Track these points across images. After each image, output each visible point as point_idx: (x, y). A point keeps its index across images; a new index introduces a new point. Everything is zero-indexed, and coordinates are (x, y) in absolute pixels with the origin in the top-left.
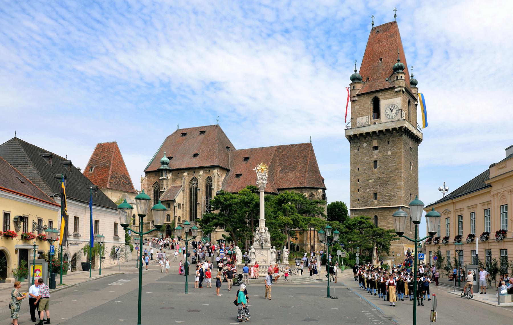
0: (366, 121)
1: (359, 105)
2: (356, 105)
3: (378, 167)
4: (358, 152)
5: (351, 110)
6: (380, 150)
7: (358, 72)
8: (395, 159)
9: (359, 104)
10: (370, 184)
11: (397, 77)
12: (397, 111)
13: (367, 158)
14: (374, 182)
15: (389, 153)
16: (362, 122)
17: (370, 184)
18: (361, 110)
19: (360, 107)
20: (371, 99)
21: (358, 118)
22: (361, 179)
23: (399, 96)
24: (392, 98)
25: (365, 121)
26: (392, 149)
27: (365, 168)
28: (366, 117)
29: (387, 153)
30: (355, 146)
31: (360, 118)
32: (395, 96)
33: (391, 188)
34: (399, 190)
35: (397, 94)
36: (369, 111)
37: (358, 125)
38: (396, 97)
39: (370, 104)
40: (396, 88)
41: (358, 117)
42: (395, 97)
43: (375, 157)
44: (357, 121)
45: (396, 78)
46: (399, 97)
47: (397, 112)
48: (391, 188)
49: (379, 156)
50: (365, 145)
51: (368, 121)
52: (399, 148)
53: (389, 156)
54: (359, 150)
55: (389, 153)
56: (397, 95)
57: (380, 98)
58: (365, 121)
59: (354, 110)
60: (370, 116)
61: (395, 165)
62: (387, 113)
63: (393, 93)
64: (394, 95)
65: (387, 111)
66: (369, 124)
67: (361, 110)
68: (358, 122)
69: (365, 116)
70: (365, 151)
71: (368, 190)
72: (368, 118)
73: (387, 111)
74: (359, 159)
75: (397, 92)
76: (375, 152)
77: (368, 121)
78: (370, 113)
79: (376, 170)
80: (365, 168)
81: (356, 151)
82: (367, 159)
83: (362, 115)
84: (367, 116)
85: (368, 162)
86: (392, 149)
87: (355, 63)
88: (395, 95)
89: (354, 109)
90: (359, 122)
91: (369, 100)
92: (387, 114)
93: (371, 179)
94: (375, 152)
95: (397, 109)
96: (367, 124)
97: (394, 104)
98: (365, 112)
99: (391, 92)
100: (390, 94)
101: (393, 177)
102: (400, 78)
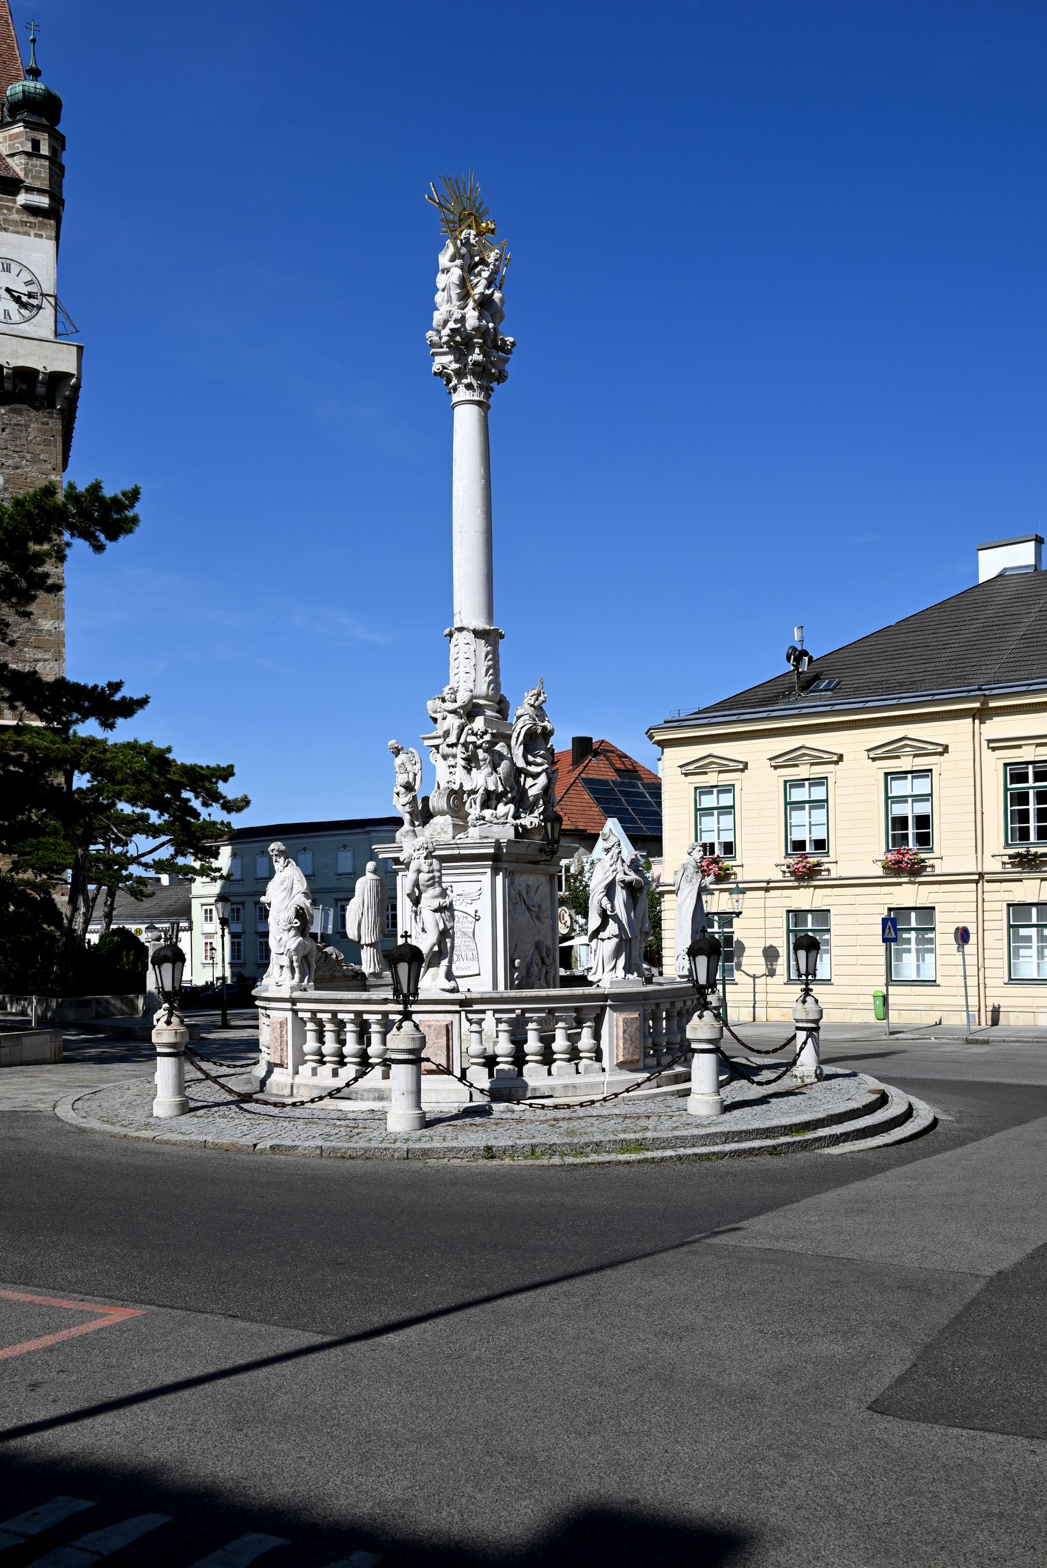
11: (36, 144)
23: (43, 233)
26: (10, 462)
32: (22, 228)
34: (47, 657)
35: (31, 219)
40: (29, 190)
42: (20, 229)
45: (28, 147)
46: (41, 236)
52: (49, 466)
56: (32, 226)
64: (15, 216)
75: (31, 210)
86: (10, 462)
88: (24, 223)
102: (45, 150)
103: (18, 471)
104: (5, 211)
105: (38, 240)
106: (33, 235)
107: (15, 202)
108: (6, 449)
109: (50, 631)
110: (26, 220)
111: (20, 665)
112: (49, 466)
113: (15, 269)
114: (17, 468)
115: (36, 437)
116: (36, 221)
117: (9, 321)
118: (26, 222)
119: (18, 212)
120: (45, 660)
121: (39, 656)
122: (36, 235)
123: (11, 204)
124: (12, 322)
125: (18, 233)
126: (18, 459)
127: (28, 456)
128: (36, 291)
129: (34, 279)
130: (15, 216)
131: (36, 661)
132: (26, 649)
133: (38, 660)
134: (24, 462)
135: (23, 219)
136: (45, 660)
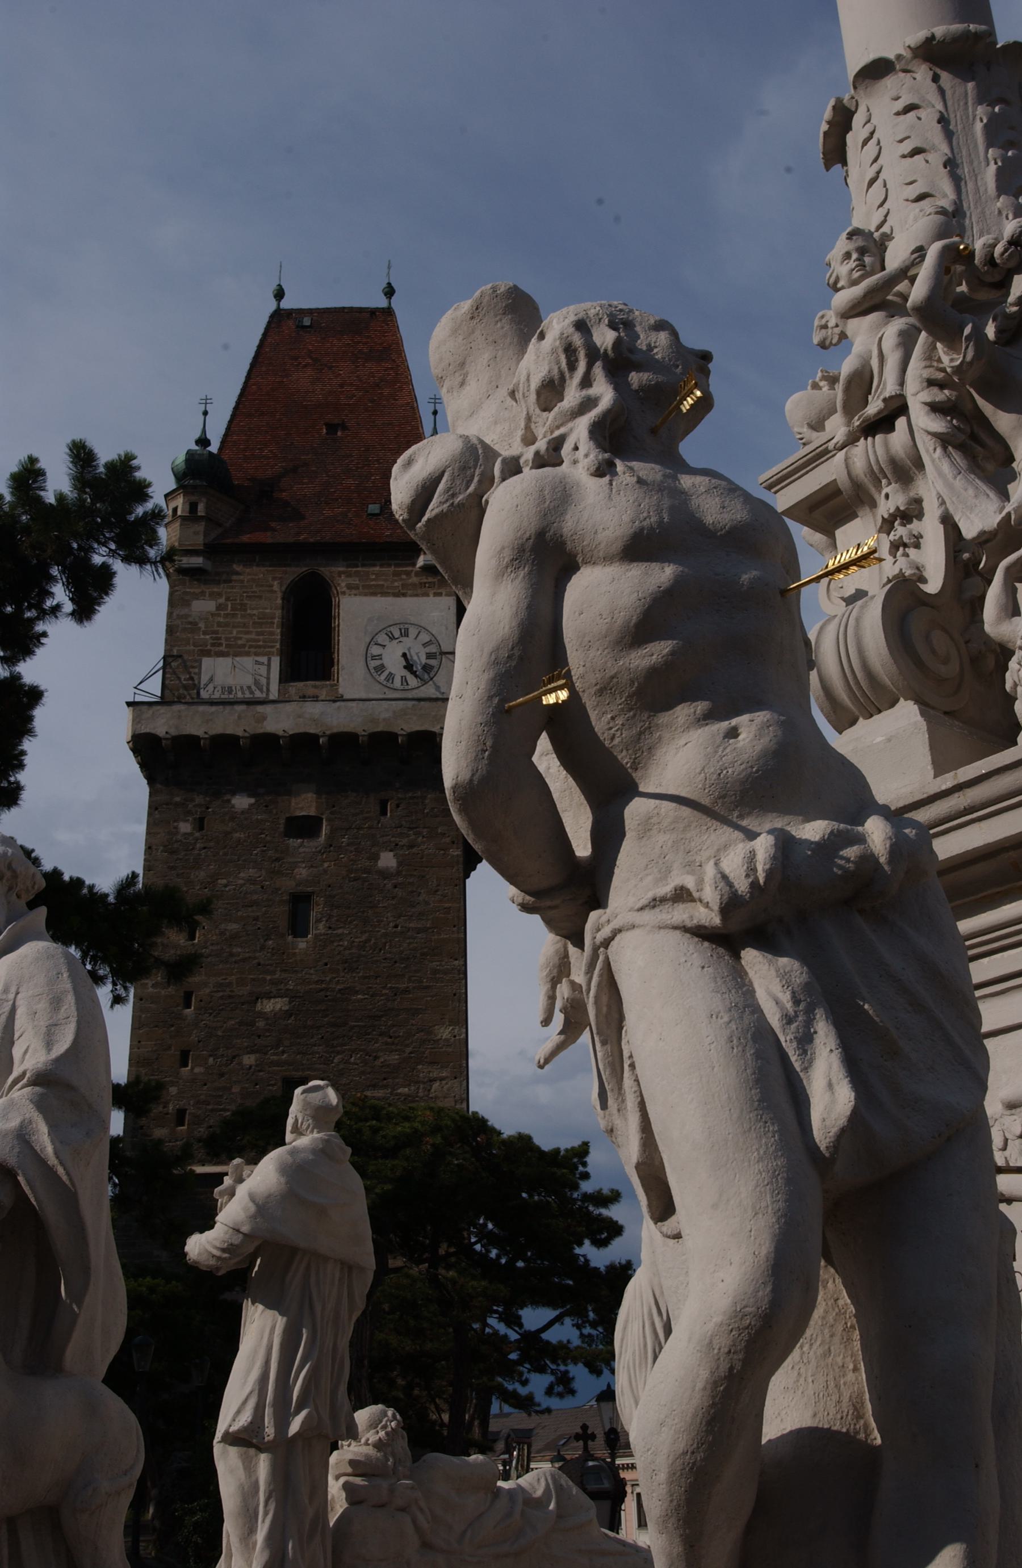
0: (257, 683)
1: (213, 596)
2: (197, 596)
3: (318, 928)
4: (197, 834)
5: (170, 615)
6: (330, 837)
7: (214, 448)
8: (421, 898)
9: (220, 595)
10: (261, 1024)
12: (430, 656)
13: (252, 872)
14: (288, 1014)
15: (387, 860)
16: (230, 681)
17: (261, 1024)
18: (227, 625)
19: (219, 607)
20: (289, 578)
21: (207, 662)
22: (208, 991)
24: (404, 595)
25: (249, 680)
26: (404, 841)
27: (234, 927)
28: (257, 663)
29: (376, 857)
30: (178, 799)
31: (220, 660)
32: (420, 590)
33: (394, 1058)
35: (430, 580)
36: (272, 633)
37: (204, 695)
38: (427, 595)
39: (279, 601)
41: (208, 654)
42: (419, 591)
43: (303, 872)
44: (199, 674)
46: (440, 594)
47: (433, 662)
48: (394, 1058)
49: (325, 871)
50: (241, 802)
51: (264, 681)
52: (448, 840)
53: (384, 874)
54: (200, 824)
55: (387, 860)
57: (343, 583)
58: (249, 680)
59: (187, 616)
60: (276, 662)
61: (419, 931)
62: (374, 657)
63: (408, 574)
64: (414, 579)
65: (375, 650)
66: (274, 695)
67: (227, 625)
68: (204, 678)
69: (248, 654)
70: (237, 835)
71: (249, 1060)
72: (263, 670)
73: (375, 650)
74: (202, 874)
76: (301, 845)
77: (264, 681)
78: (278, 646)
79: (302, 944)
80: (234, 927)
81: (185, 827)
82: (251, 881)
83: (235, 650)
84: (264, 659)
85: (255, 897)
86: (404, 841)
87: (202, 408)
88: (422, 585)
89: (185, 611)
90: (211, 680)
91: (276, 583)
92: (378, 663)
93: (269, 996)
94: (301, 845)
95: (433, 649)
96: (258, 694)
97: (413, 620)
98: (253, 636)
99: (396, 565)
100: (396, 574)
101: (406, 991)
103: (415, 850)
104: (404, 577)
105: (438, 599)
106: (431, 595)
107: (414, 565)
108: (401, 826)
109: (447, 1040)
110: (425, 581)
111: (413, 1088)
112: (448, 840)
113: (413, 632)
114: (411, 846)
115: (433, 808)
116: (436, 580)
117: (406, 687)
118: (425, 583)
119: (417, 574)
120: (442, 1079)
121: (434, 1074)
122: (436, 594)
123: (409, 569)
124: (410, 687)
125: (417, 595)
126: (413, 837)
127: (425, 832)
128: (434, 651)
129: (433, 639)
130: (414, 579)
131: (431, 1081)
132: (420, 1067)
133: (434, 1080)
134: (420, 839)
135: (422, 581)
136: (442, 1079)
